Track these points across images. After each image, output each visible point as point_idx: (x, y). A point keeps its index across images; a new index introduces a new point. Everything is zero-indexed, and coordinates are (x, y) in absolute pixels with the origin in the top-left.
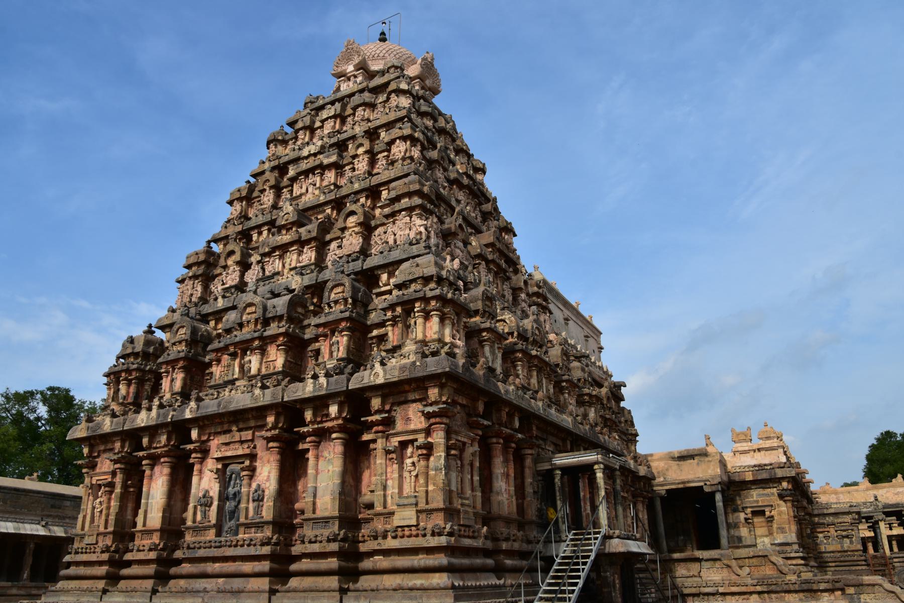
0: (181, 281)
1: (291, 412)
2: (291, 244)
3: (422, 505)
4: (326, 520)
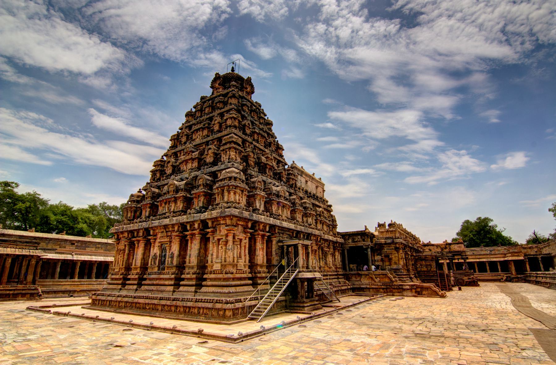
1: (183, 226)
2: (190, 159)
3: (223, 263)
4: (193, 268)
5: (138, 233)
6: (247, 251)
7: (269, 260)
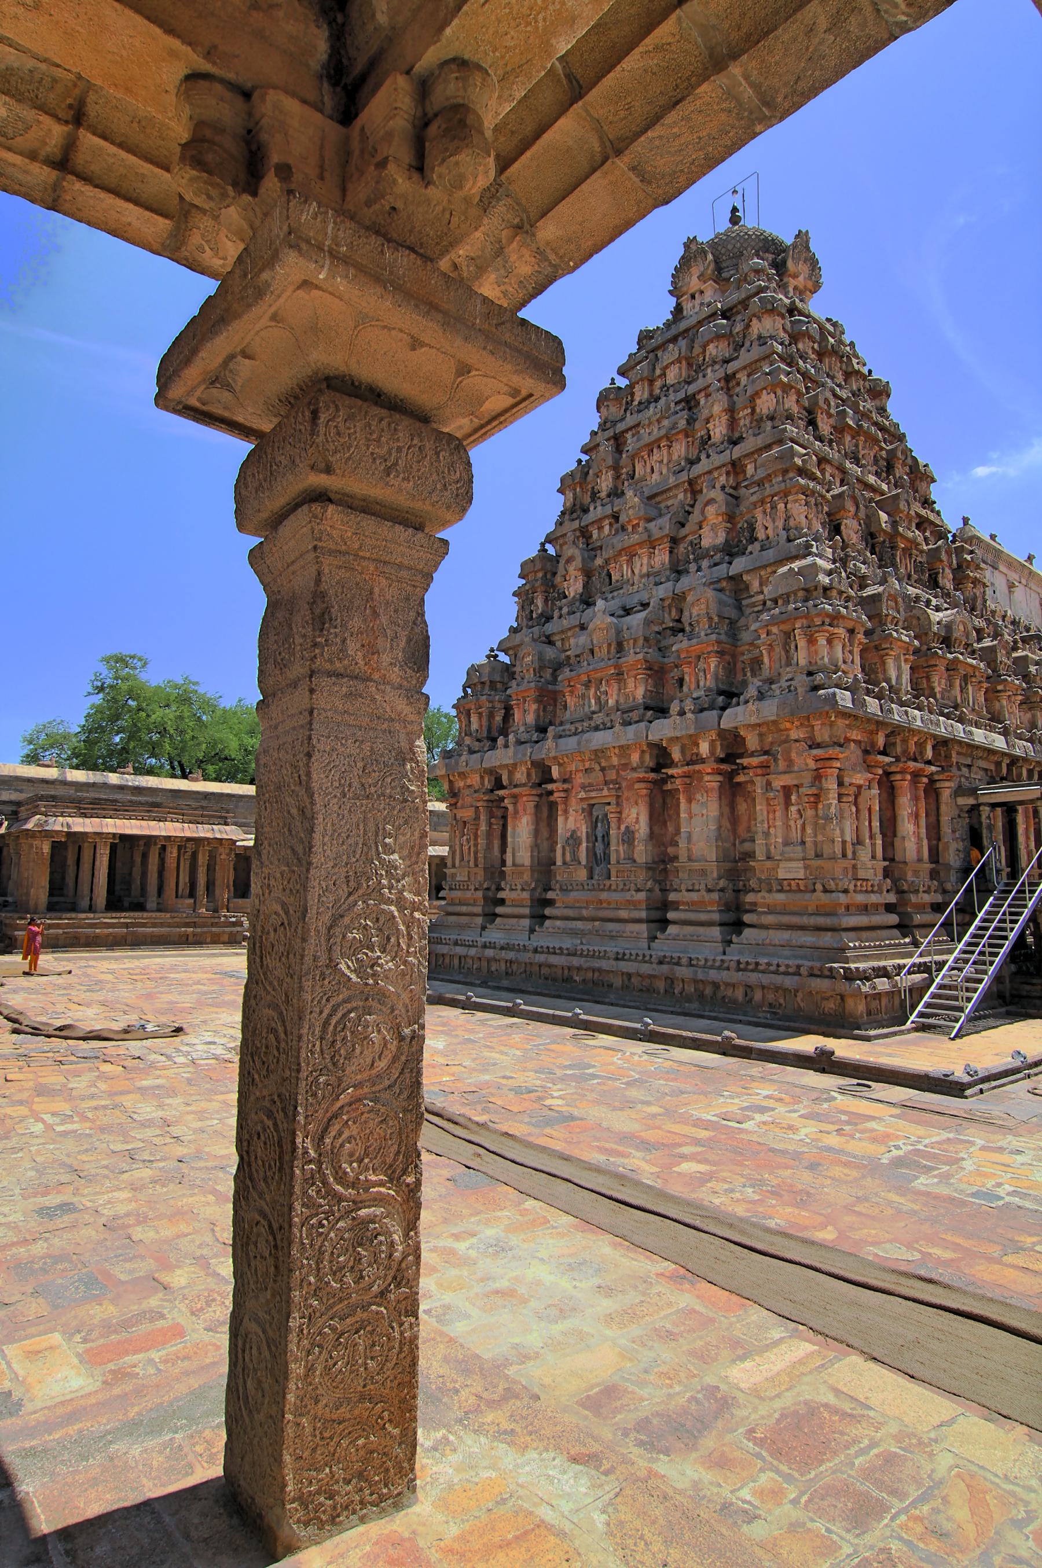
2: (640, 544)
5: (511, 774)
6: (876, 824)
7: (935, 855)
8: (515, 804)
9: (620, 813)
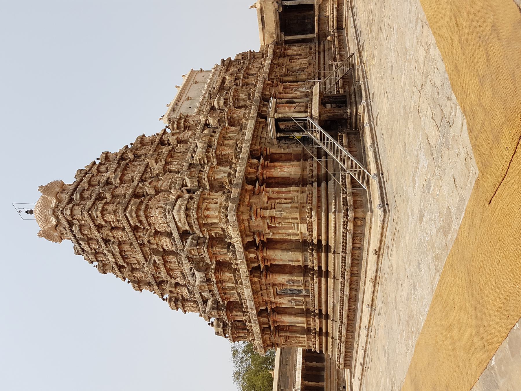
0: (185, 311)
1: (254, 271)
2: (165, 266)
3: (298, 221)
5: (264, 323)
6: (284, 190)
7: (298, 157)
8: (277, 322)
9: (280, 284)
